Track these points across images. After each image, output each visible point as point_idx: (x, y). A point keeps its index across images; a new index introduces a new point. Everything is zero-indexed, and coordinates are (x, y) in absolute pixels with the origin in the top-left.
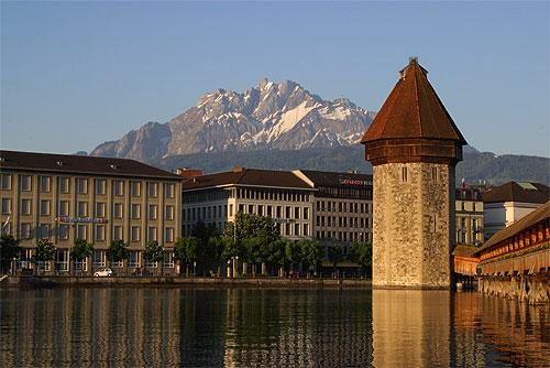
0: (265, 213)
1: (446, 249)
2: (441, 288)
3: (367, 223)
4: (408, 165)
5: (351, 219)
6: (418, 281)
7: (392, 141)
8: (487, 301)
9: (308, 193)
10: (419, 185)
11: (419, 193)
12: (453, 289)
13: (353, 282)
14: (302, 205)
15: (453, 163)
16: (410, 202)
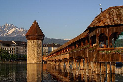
0: (6, 49)
1: (41, 56)
2: (40, 63)
3: (26, 51)
4: (34, 40)
5: (23, 50)
6: (36, 62)
7: (31, 35)
8: (48, 65)
9: (15, 45)
10: (36, 44)
11: (36, 45)
12: (42, 63)
13: (23, 62)
14: (13, 48)
15: (42, 40)
16: (34, 47)
